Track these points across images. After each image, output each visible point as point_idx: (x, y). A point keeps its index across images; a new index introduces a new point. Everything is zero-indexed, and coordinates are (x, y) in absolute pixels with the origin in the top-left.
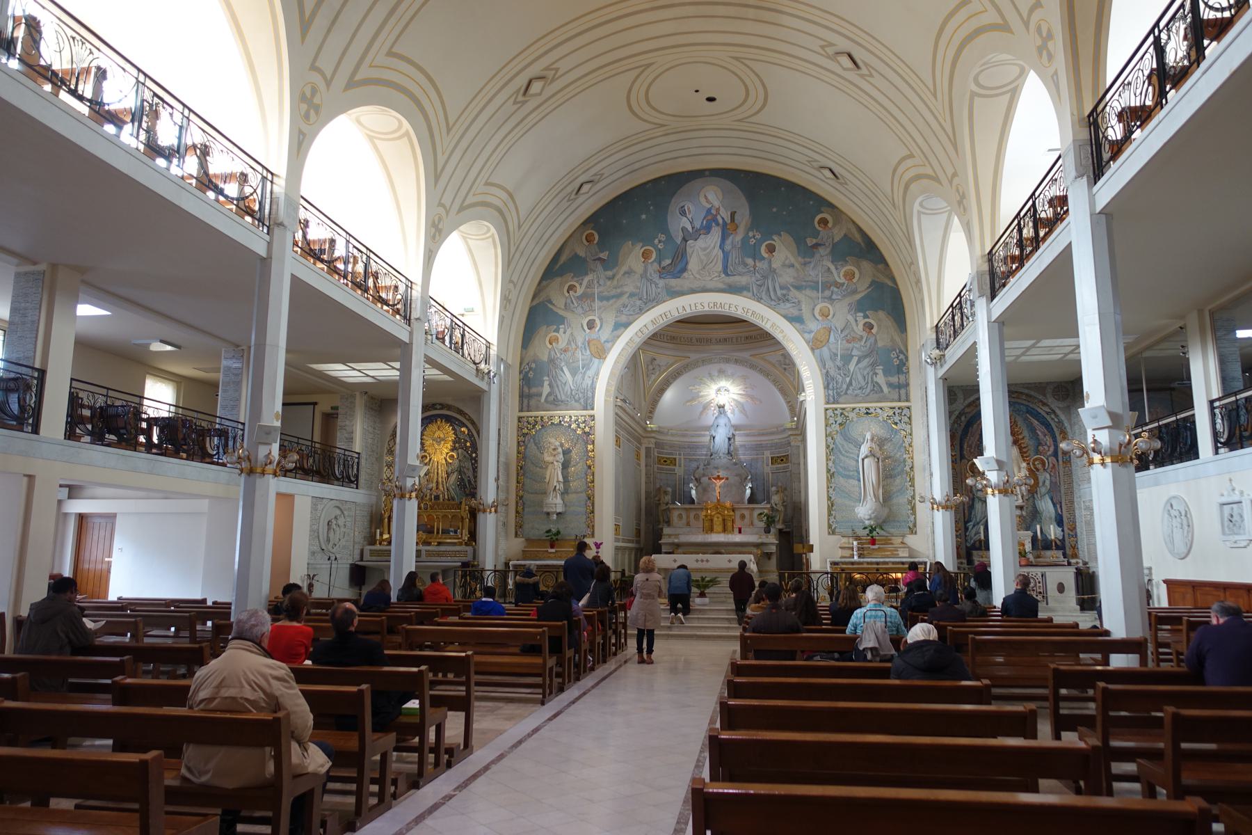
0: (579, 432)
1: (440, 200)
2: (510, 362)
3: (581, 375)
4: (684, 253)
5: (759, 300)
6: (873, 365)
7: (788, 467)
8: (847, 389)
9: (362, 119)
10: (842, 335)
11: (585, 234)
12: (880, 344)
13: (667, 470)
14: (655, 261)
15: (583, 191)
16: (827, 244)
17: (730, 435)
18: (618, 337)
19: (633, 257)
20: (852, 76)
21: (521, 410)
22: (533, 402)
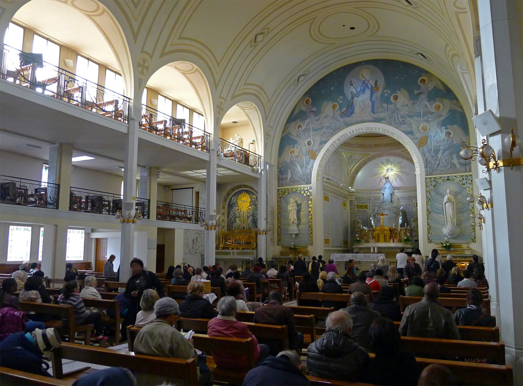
0: (305, 195)
1: (220, 95)
2: (273, 163)
3: (305, 168)
4: (352, 105)
5: (390, 124)
6: (451, 154)
8: (437, 167)
9: (177, 66)
10: (434, 139)
11: (305, 100)
12: (455, 143)
13: (362, 211)
14: (338, 110)
15: (300, 80)
16: (425, 92)
18: (322, 148)
19: (328, 108)
20: (410, 8)
21: (279, 186)
22: (284, 182)
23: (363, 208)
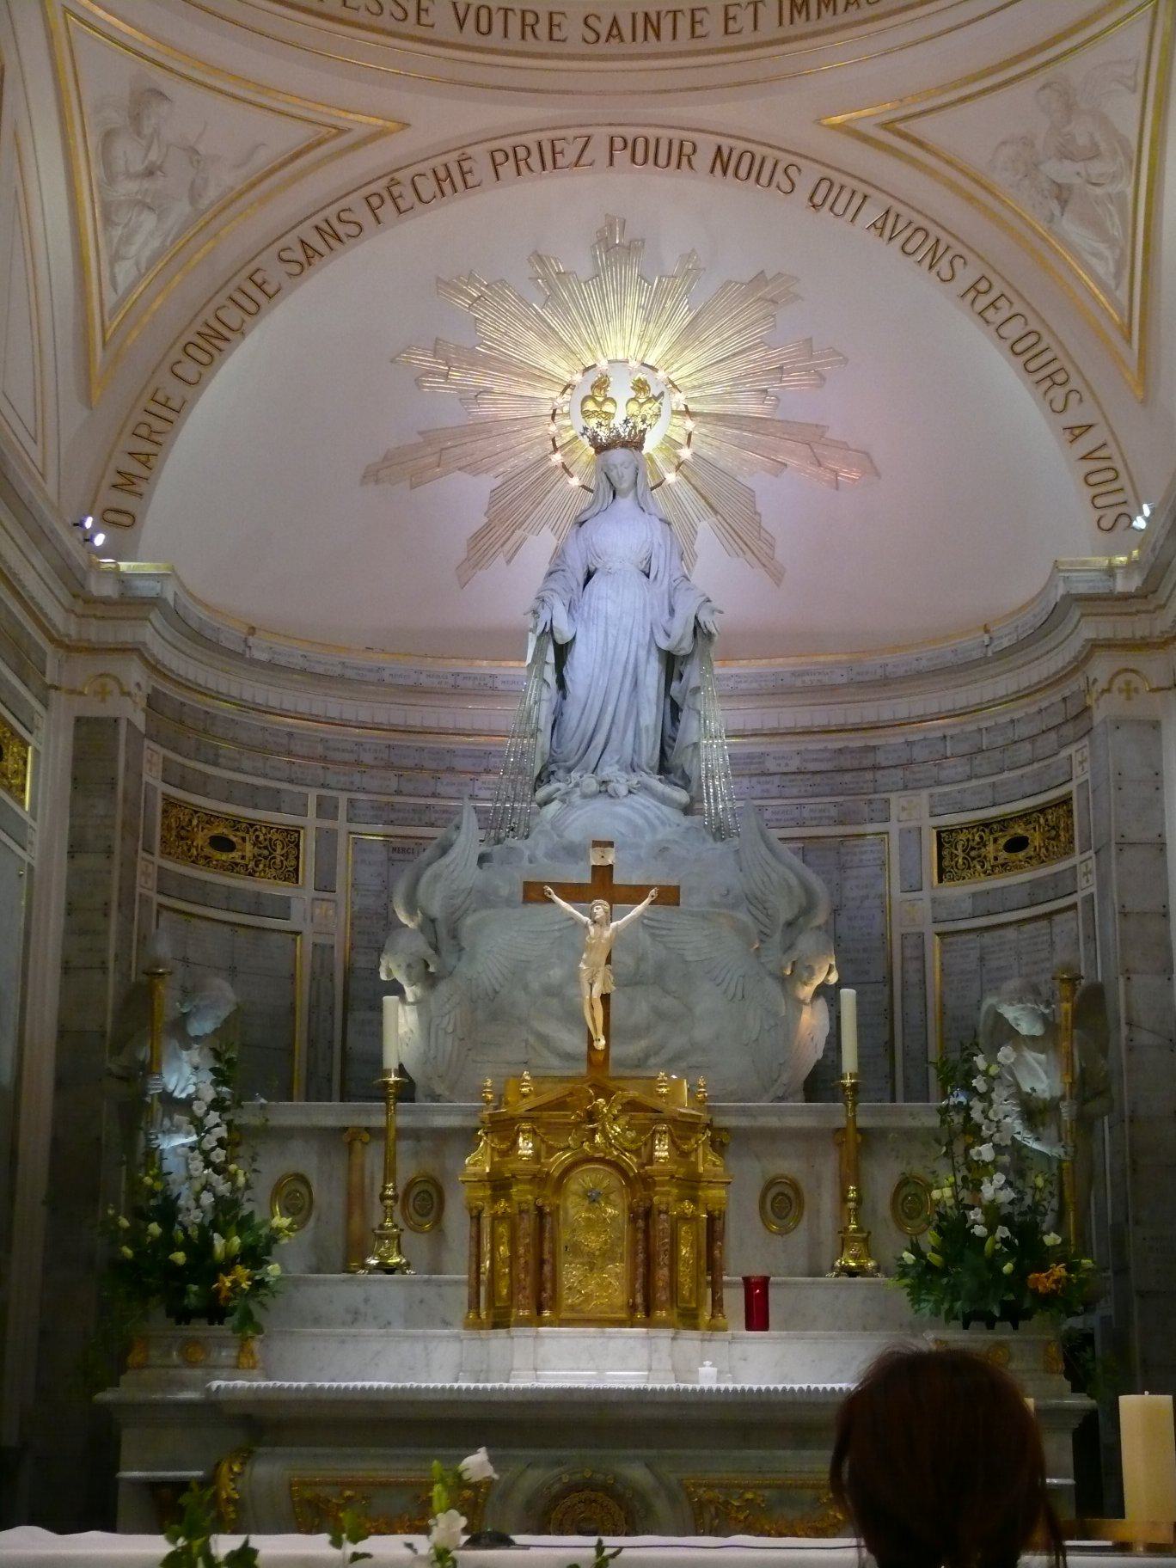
7: (1062, 885)
17: (679, 636)
23: (232, 867)
